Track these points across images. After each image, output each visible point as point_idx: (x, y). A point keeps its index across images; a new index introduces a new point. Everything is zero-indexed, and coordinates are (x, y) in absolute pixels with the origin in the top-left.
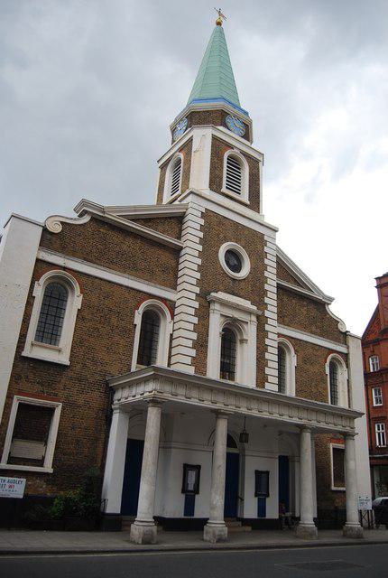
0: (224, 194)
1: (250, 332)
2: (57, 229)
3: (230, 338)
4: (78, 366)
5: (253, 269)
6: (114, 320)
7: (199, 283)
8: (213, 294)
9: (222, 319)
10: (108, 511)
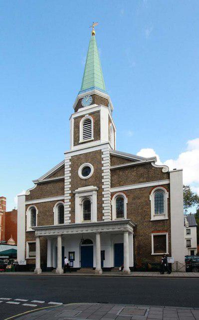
0: (82, 143)
2: (29, 193)
3: (87, 205)
8: (76, 190)
9: (80, 198)
10: (48, 267)
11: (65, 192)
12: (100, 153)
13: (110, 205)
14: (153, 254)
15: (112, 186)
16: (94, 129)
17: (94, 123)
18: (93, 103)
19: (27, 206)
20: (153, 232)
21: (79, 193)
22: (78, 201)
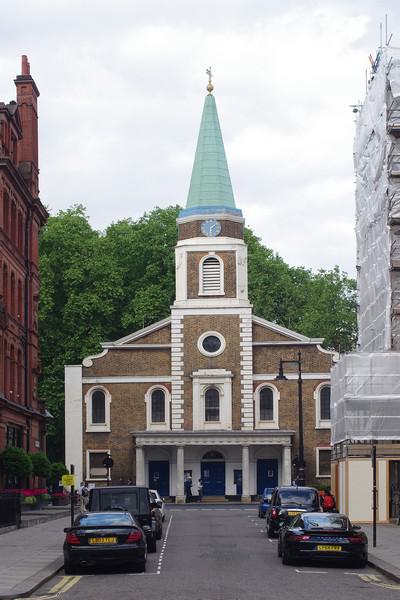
1: (226, 391)
3: (212, 396)
4: (116, 432)
5: (229, 345)
6: (132, 403)
7: (183, 368)
8: (195, 373)
11: (173, 373)
12: (237, 319)
13: (250, 399)
14: (318, 476)
15: (255, 371)
20: (318, 445)
21: (201, 377)
22: (198, 391)
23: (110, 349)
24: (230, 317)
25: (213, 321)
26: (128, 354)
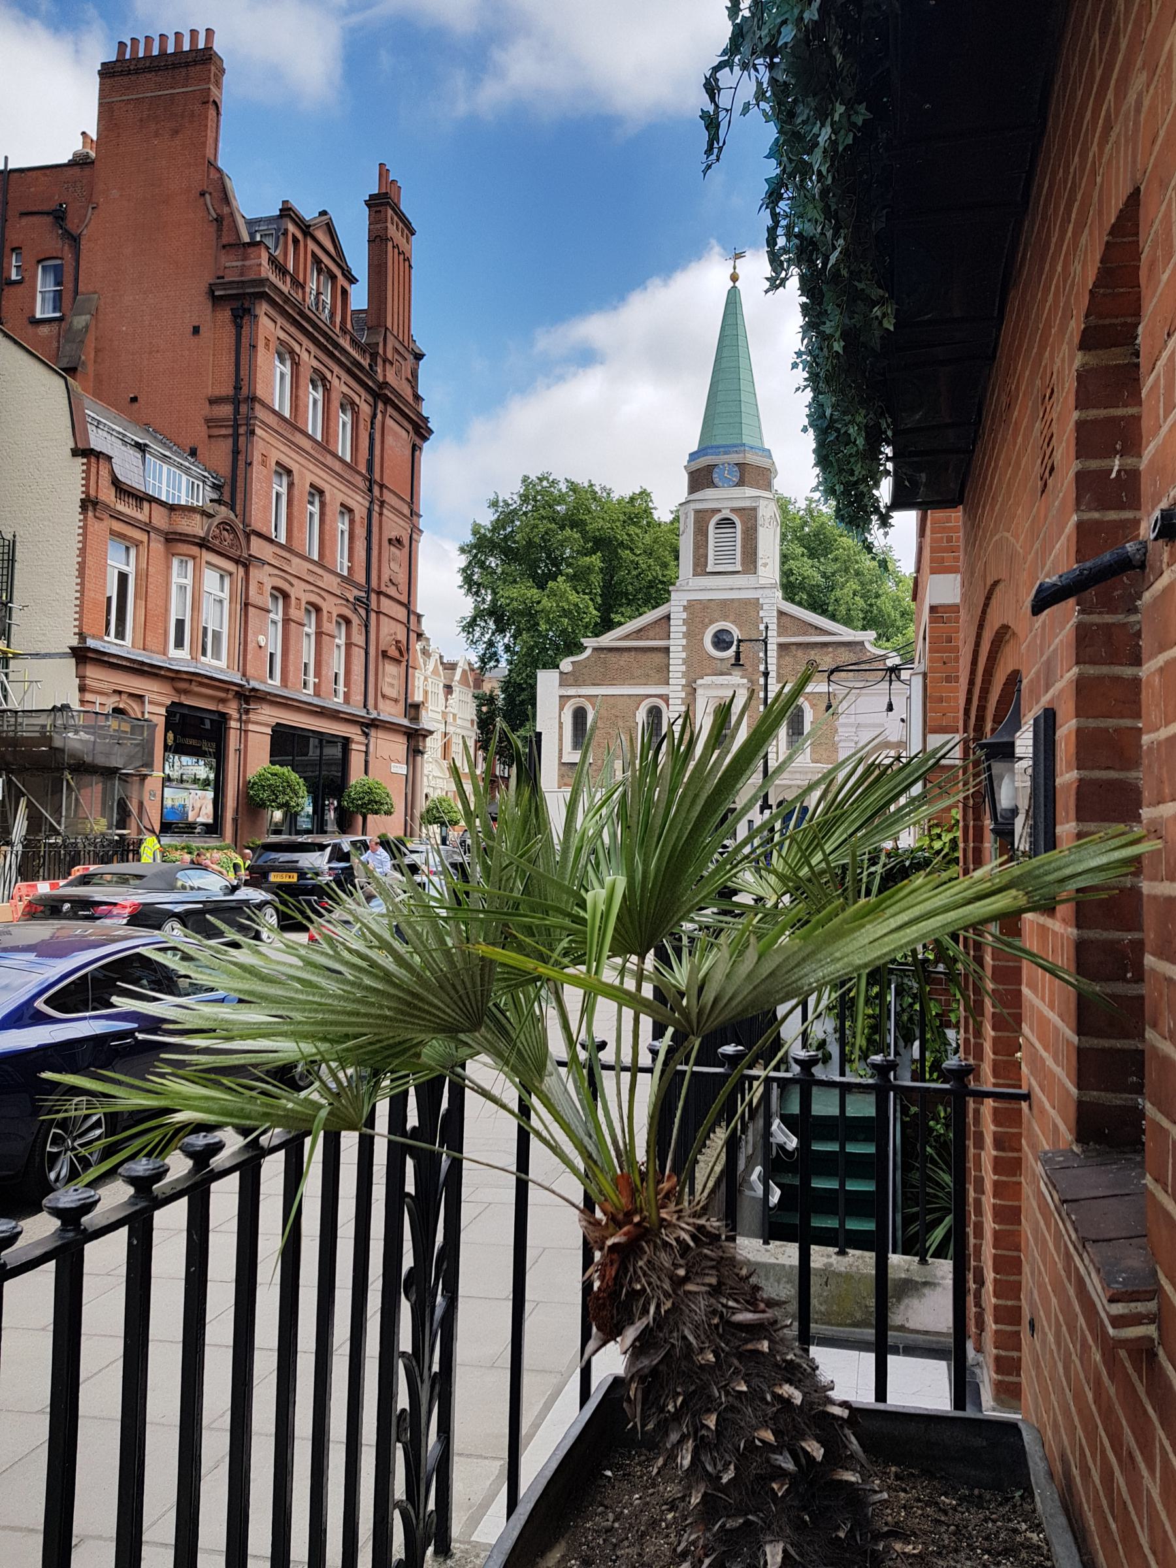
6: (621, 724)
7: (685, 674)
8: (699, 682)
12: (756, 604)
16: (743, 547)
17: (743, 532)
18: (741, 483)
19: (564, 699)
23: (595, 649)
24: (746, 602)
25: (725, 607)
26: (617, 655)
